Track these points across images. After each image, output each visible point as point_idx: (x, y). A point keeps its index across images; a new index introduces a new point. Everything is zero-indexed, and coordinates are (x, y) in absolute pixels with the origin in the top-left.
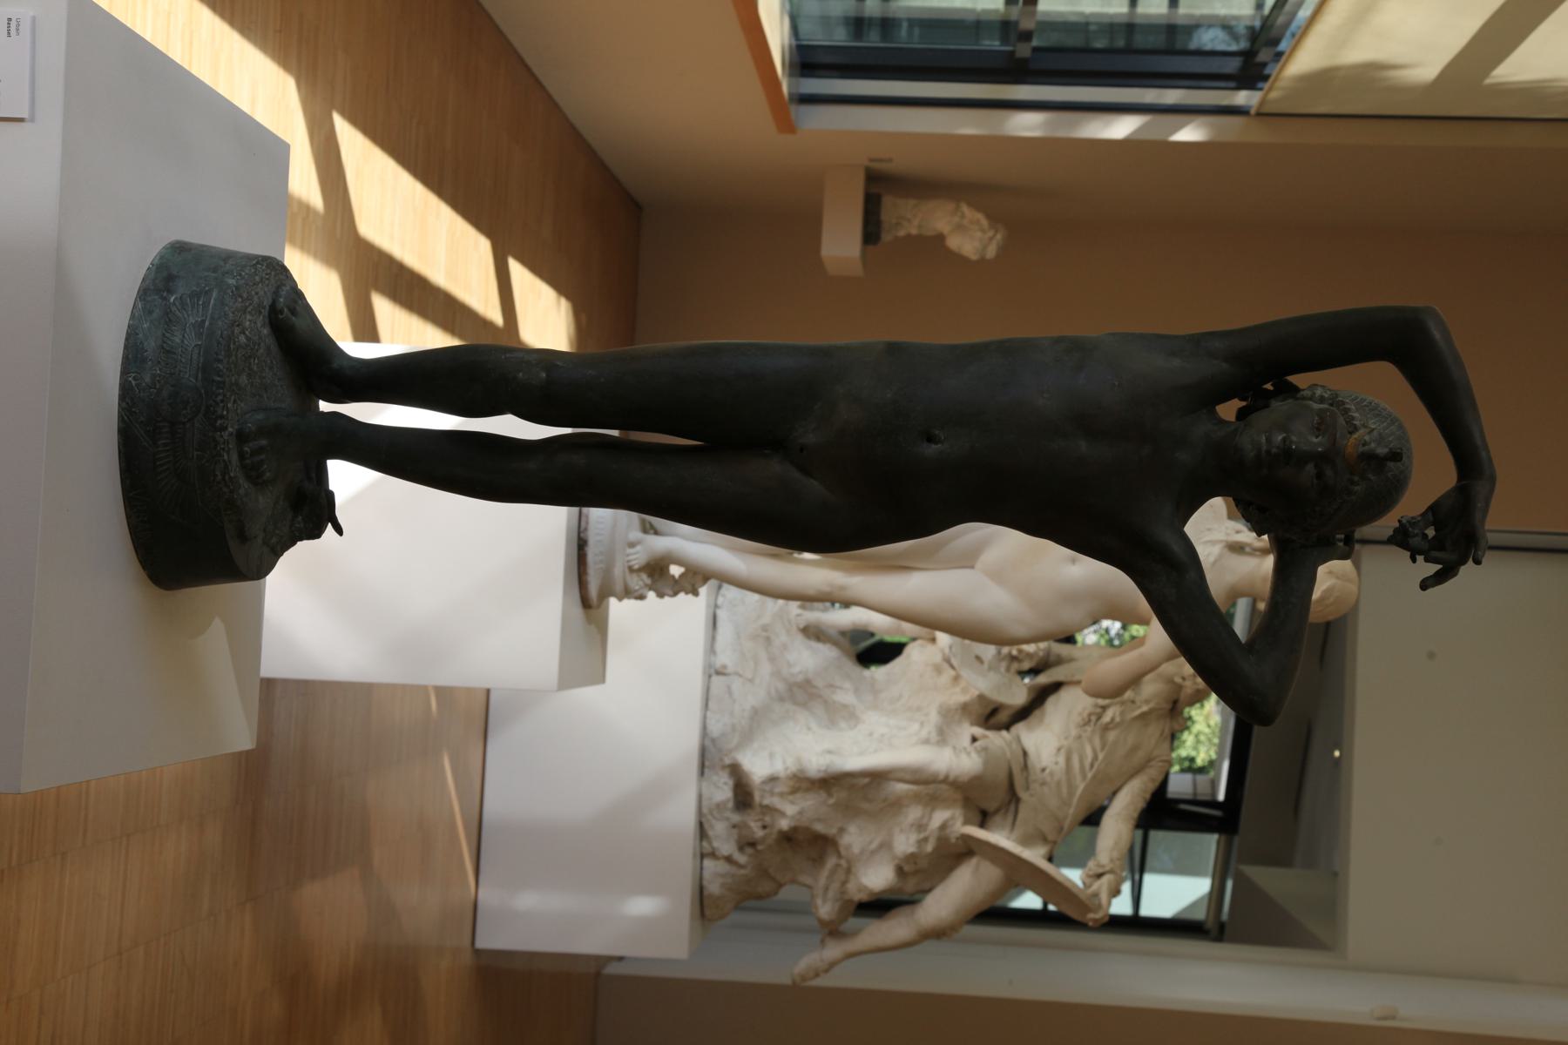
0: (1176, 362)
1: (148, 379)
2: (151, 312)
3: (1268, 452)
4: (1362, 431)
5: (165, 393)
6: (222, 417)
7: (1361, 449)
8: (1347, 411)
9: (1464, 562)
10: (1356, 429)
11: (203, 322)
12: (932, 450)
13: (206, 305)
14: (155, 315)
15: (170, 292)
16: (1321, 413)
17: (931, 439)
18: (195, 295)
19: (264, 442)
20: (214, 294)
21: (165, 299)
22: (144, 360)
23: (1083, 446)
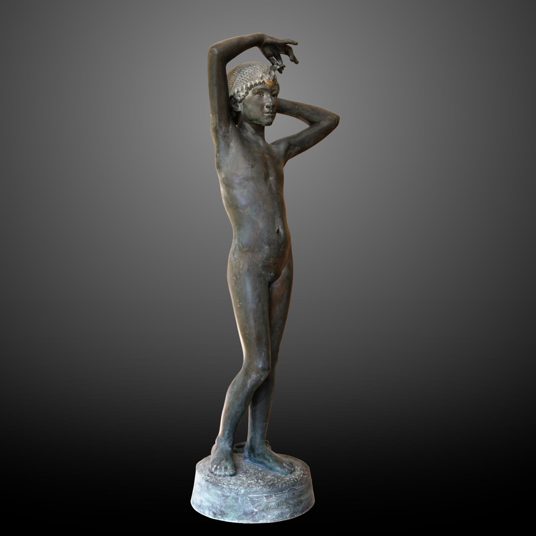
0: (232, 144)
1: (288, 510)
2: (264, 516)
3: (272, 113)
4: (265, 80)
5: (292, 502)
6: (294, 480)
7: (271, 80)
8: (256, 85)
9: (290, 48)
10: (264, 82)
11: (265, 496)
12: (281, 231)
13: (258, 498)
14: (265, 514)
15: (252, 512)
16: (254, 94)
17: (278, 231)
18: (253, 502)
19: (284, 465)
20: (251, 496)
21: (256, 513)
22: (282, 513)
23: (271, 178)
